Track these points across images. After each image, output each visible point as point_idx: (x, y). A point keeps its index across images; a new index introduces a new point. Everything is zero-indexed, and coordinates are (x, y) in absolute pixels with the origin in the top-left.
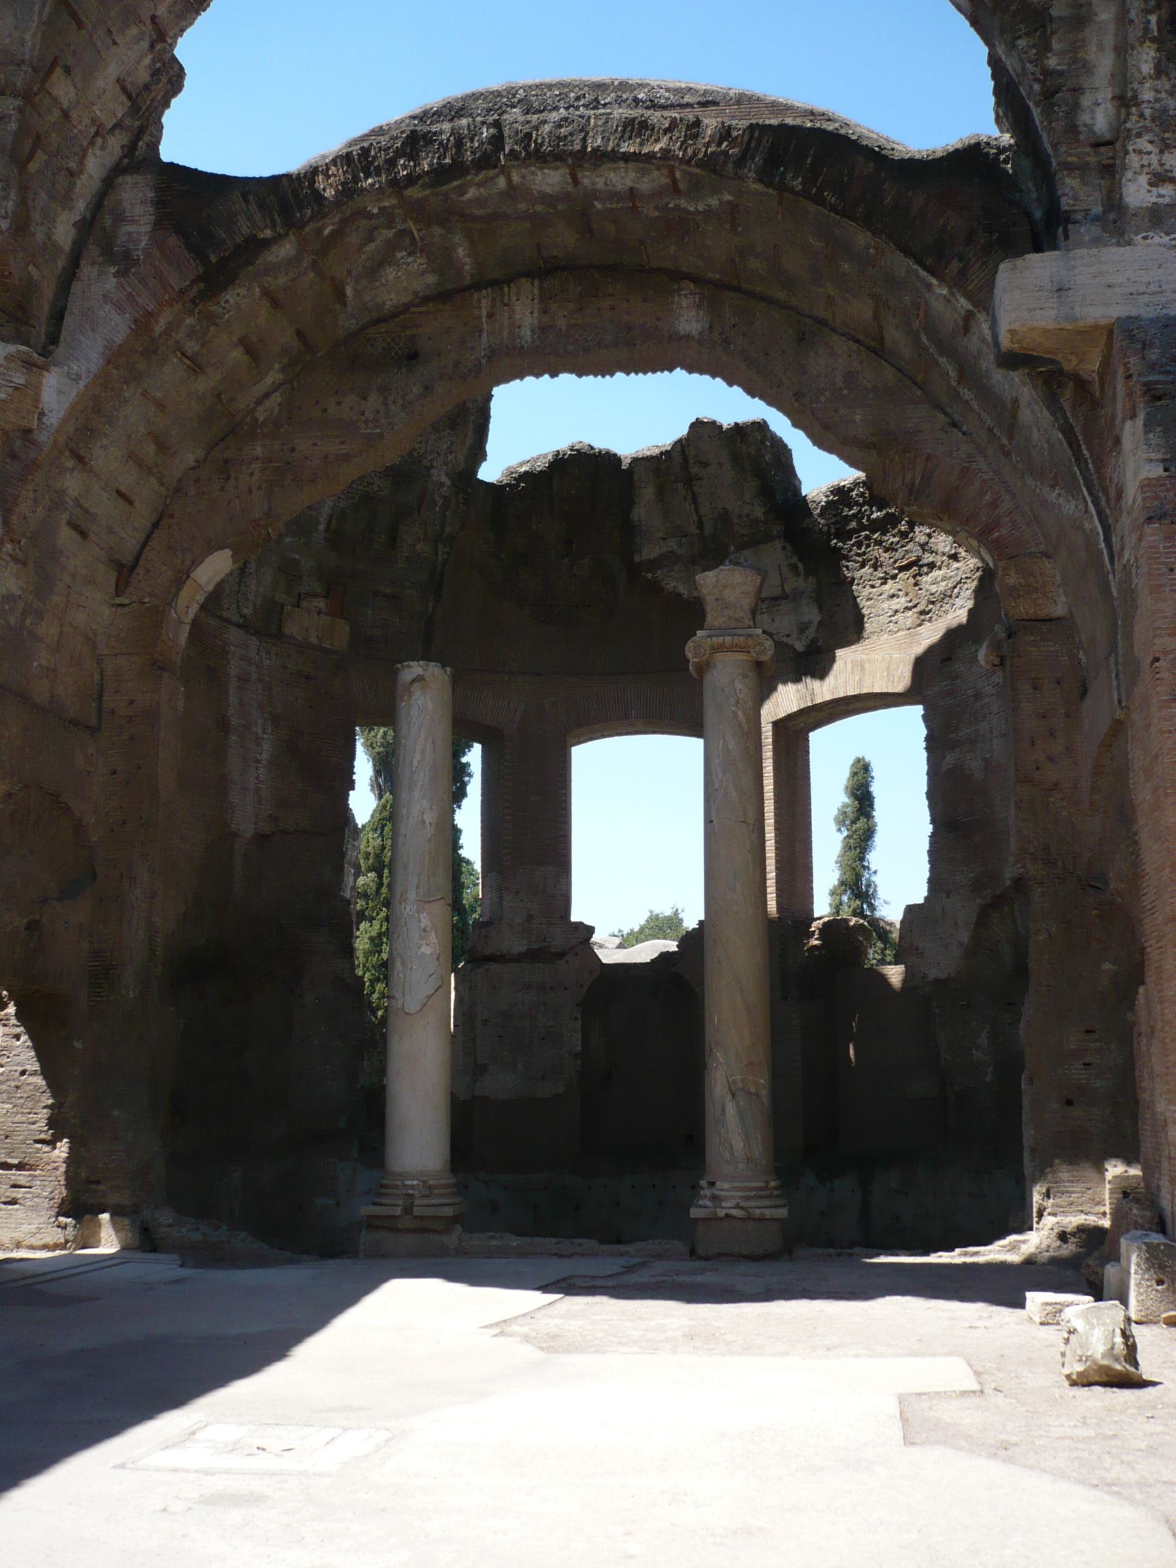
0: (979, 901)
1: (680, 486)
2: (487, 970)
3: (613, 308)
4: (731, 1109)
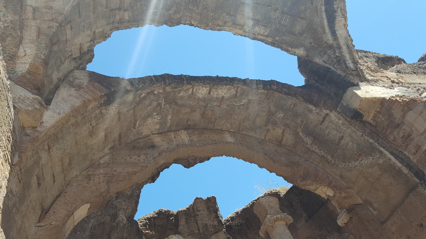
1: (192, 218)
3: (208, 136)
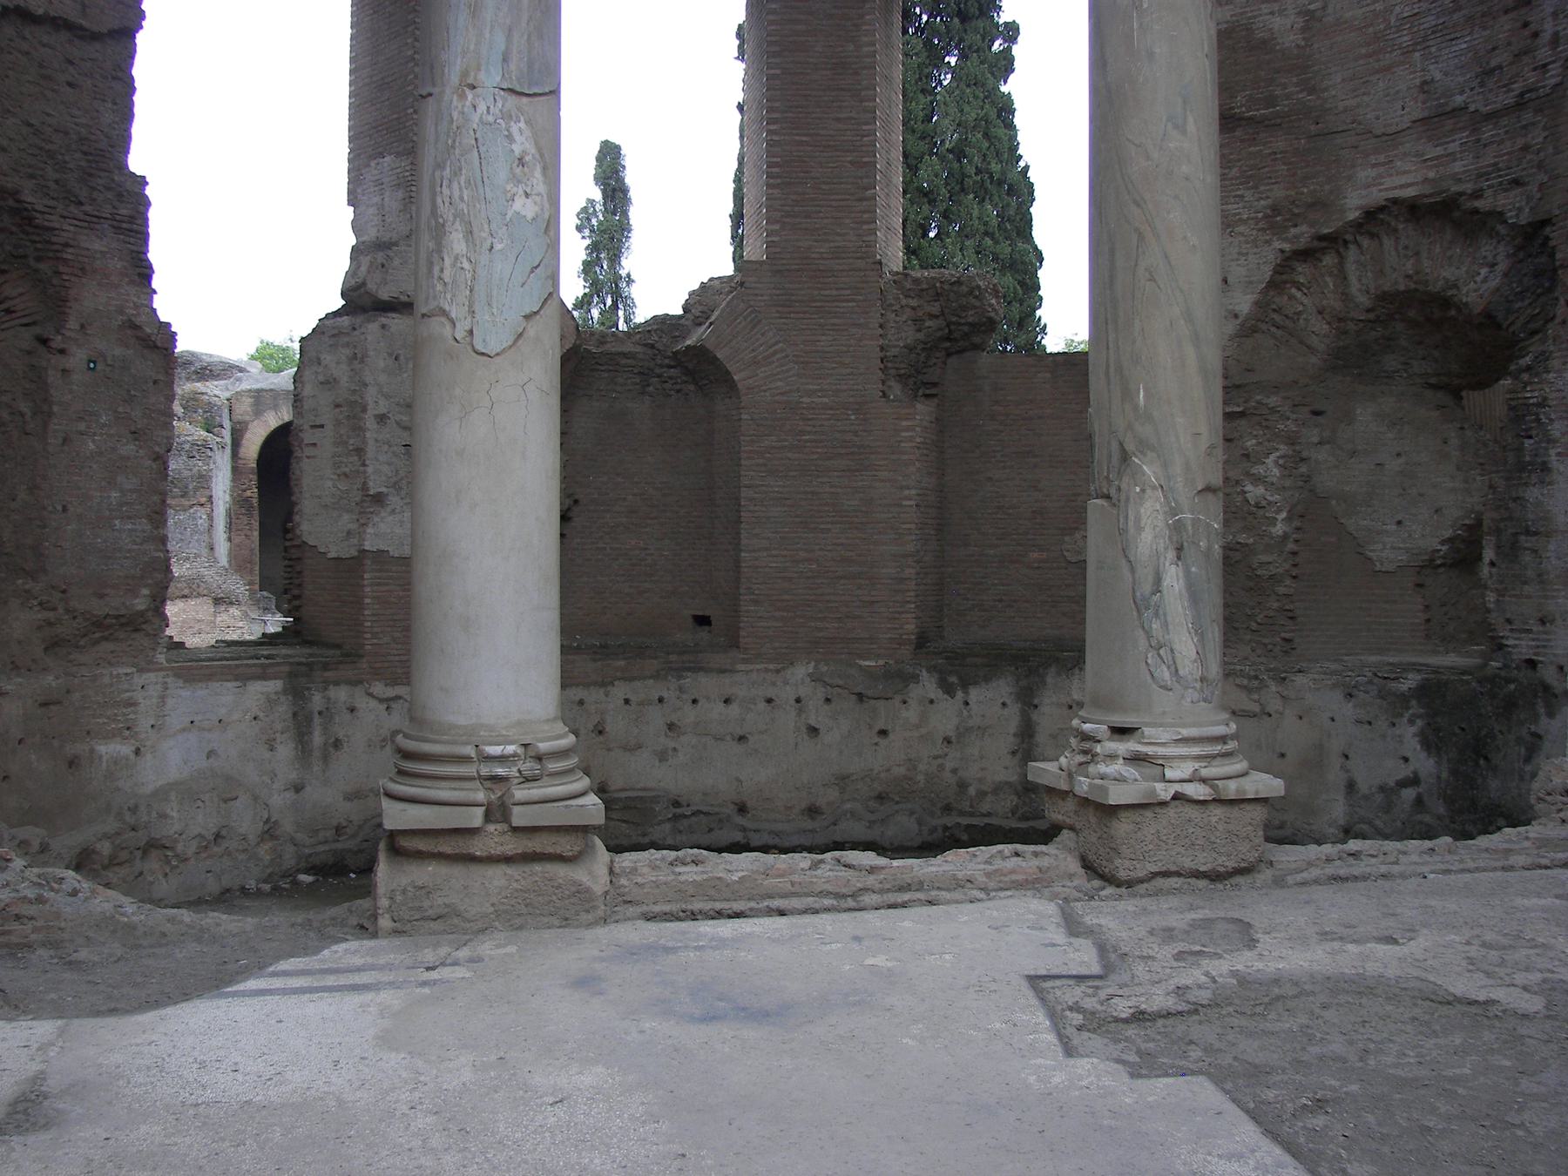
0: (1277, 245)
2: (383, 327)
4: (1173, 578)
